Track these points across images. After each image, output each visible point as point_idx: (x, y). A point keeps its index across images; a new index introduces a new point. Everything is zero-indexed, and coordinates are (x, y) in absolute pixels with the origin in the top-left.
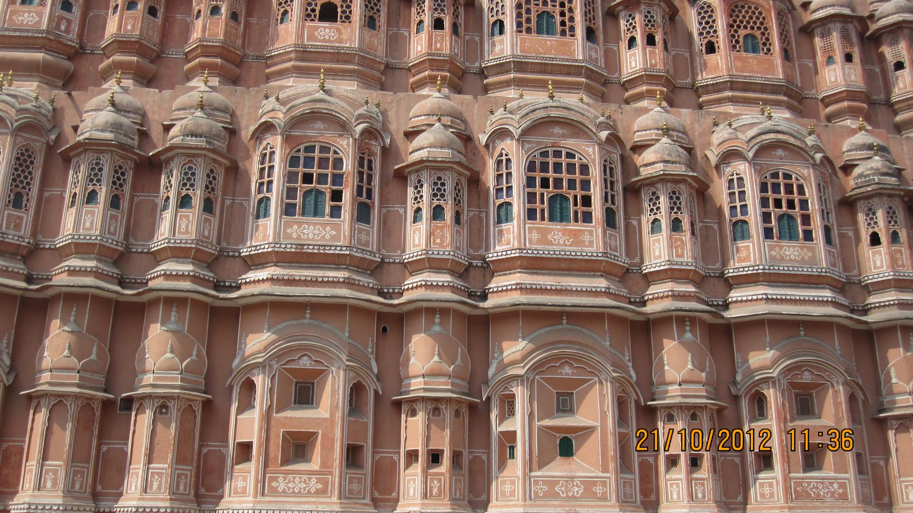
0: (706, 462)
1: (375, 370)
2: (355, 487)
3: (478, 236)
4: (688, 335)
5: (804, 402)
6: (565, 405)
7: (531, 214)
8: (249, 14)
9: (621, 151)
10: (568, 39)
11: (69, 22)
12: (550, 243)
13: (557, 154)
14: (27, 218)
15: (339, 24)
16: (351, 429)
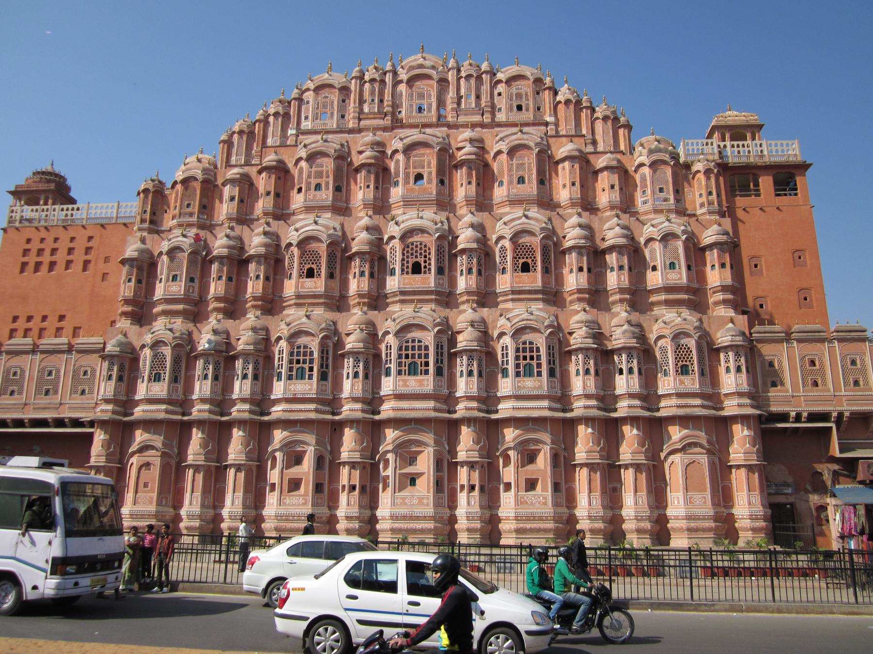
0: (477, 488)
1: (329, 448)
2: (319, 501)
3: (377, 385)
4: (472, 427)
5: (530, 457)
6: (412, 461)
7: (399, 373)
8: (275, 274)
9: (447, 335)
10: (427, 275)
11: (193, 287)
12: (408, 386)
13: (413, 341)
14: (180, 387)
15: (315, 279)
16: (316, 476)
